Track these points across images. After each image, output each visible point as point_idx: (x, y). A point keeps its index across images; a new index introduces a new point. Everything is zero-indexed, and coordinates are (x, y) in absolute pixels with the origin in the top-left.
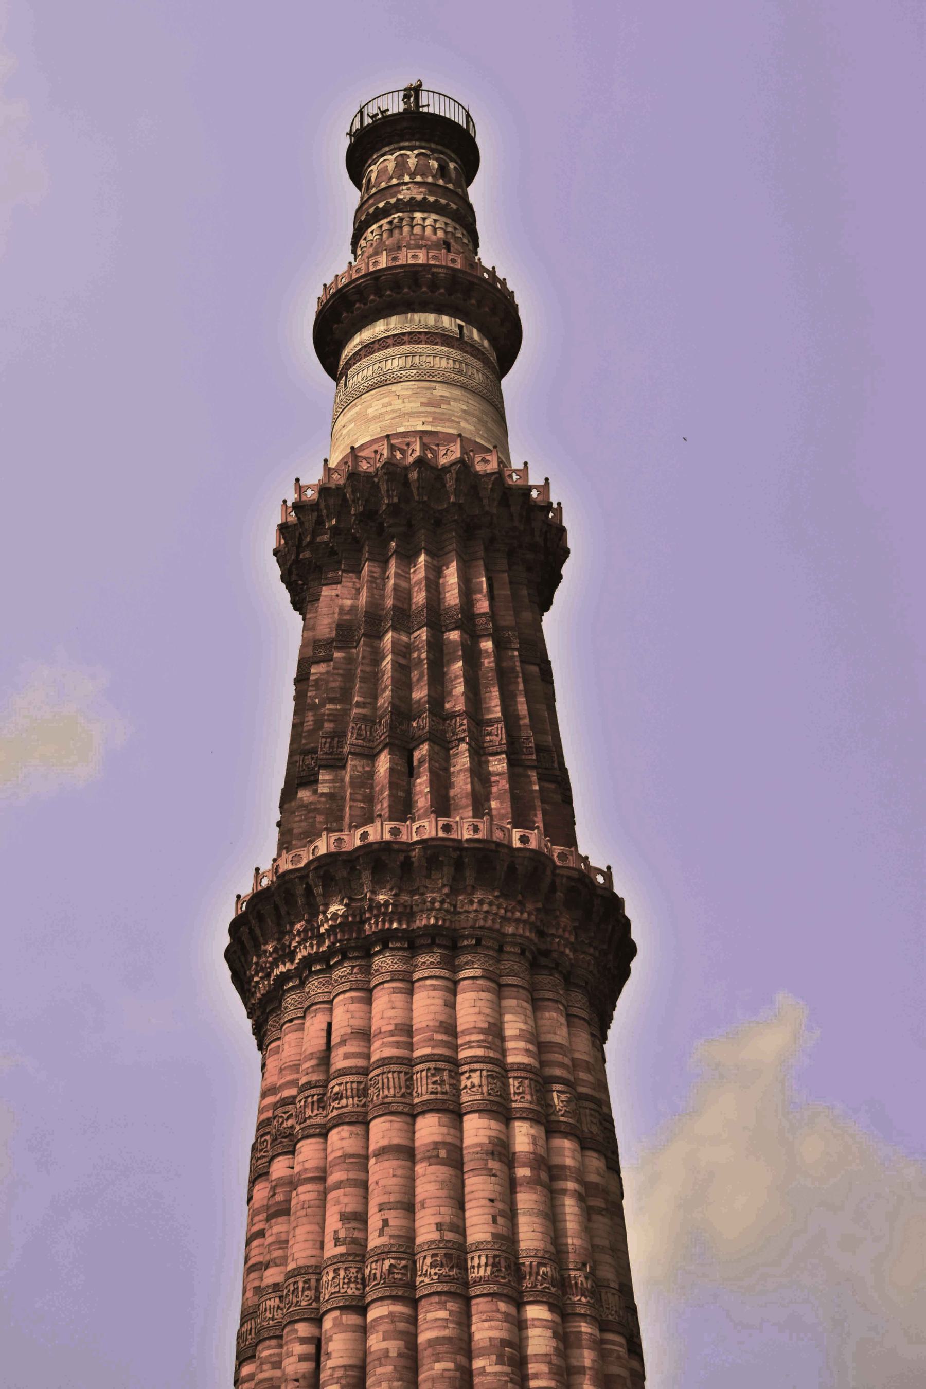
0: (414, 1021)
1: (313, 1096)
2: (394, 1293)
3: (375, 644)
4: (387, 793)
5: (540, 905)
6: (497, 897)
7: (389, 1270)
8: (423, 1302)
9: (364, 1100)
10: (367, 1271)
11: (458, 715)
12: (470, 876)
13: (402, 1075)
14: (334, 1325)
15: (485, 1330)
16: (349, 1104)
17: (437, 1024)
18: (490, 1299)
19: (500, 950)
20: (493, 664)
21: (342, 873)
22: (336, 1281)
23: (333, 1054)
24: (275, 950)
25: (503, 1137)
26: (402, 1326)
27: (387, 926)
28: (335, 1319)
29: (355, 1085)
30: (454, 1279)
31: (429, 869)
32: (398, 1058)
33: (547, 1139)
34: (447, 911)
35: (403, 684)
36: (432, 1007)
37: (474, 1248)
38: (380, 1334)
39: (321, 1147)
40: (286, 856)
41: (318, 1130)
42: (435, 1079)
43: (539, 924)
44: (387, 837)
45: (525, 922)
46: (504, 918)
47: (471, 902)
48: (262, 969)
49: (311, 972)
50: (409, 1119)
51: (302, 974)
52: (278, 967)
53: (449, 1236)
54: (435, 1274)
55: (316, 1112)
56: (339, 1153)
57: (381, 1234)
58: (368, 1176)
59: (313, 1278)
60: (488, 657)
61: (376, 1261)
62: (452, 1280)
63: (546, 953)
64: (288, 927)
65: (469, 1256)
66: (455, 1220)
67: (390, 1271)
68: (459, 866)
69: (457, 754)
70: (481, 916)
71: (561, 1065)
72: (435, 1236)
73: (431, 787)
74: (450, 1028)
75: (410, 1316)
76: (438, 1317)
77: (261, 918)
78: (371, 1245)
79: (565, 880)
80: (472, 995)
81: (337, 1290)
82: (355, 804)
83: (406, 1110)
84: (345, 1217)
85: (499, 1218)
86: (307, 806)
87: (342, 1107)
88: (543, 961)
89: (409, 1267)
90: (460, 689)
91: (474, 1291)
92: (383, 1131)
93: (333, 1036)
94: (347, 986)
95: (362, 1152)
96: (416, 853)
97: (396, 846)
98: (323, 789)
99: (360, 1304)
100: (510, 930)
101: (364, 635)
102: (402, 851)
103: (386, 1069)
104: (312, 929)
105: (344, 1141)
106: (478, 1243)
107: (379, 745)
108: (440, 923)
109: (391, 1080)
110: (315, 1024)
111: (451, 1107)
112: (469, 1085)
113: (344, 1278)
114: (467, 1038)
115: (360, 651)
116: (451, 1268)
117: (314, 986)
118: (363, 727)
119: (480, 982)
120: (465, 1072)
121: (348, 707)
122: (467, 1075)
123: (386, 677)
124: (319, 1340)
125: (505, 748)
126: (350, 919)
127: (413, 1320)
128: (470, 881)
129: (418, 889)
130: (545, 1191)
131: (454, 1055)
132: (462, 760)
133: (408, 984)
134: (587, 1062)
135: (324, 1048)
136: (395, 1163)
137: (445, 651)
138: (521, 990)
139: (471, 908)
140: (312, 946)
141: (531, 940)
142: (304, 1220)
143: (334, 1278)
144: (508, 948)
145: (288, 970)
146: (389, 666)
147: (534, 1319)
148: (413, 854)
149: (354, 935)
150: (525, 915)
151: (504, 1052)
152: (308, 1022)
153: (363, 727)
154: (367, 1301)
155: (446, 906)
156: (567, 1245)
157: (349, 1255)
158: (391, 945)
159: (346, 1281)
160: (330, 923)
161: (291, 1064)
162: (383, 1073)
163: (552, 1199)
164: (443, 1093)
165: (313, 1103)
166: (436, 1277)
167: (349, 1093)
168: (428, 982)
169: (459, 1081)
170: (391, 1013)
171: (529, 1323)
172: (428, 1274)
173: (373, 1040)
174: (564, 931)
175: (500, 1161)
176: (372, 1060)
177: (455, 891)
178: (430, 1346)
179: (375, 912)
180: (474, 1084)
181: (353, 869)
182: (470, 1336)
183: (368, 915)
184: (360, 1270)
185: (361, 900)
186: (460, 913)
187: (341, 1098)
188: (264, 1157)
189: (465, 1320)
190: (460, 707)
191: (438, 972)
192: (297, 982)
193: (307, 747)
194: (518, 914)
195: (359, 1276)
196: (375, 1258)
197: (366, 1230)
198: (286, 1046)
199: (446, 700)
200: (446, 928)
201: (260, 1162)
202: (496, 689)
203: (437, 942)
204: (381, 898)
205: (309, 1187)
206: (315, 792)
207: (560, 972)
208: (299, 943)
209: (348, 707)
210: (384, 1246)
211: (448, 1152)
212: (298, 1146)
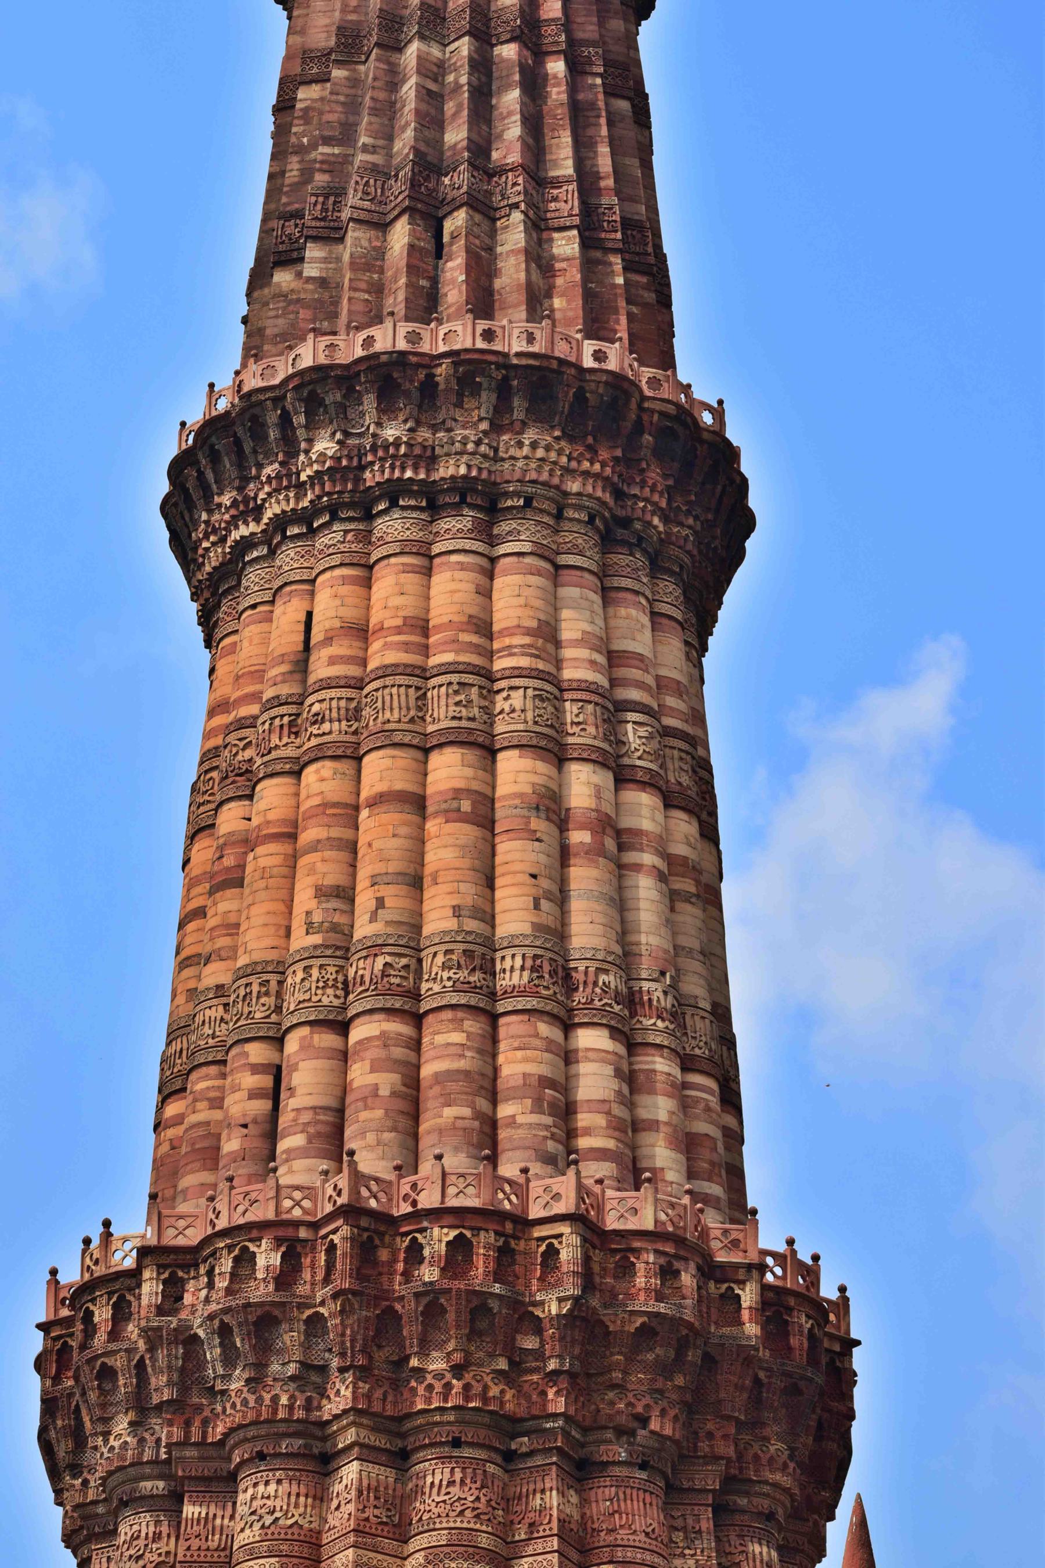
0: (433, 614)
1: (282, 716)
2: (388, 1005)
3: (392, 59)
4: (403, 281)
5: (619, 453)
6: (557, 438)
7: (383, 971)
8: (430, 1019)
9: (356, 725)
11: (511, 170)
12: (519, 406)
13: (412, 691)
14: (302, 1048)
15: (517, 1064)
16: (335, 730)
17: (465, 619)
18: (526, 1017)
19: (559, 516)
20: (564, 97)
21: (334, 396)
22: (307, 984)
23: (312, 659)
24: (235, 503)
25: (555, 788)
26: (399, 1052)
27: (397, 474)
28: (303, 1039)
29: (343, 703)
30: (476, 987)
31: (460, 395)
32: (406, 666)
33: (617, 790)
34: (485, 456)
35: (432, 120)
36: (457, 595)
37: (505, 944)
38: (367, 1063)
39: (292, 790)
40: (254, 367)
41: (288, 766)
42: (458, 698)
43: (616, 479)
44: (402, 345)
45: (597, 476)
46: (567, 470)
47: (520, 444)
48: (215, 531)
49: (284, 537)
50: (419, 755)
51: (271, 539)
52: (237, 527)
53: (471, 925)
54: (449, 979)
55: (285, 740)
56: (316, 801)
57: (373, 918)
58: (357, 834)
59: (274, 979)
60: (558, 85)
61: (366, 957)
62: (474, 989)
63: (625, 523)
64: (254, 471)
65: (499, 955)
66: (480, 902)
67: (384, 974)
68: (504, 392)
69: (507, 227)
70: (533, 466)
71: (640, 685)
72: (452, 924)
73: (468, 275)
74: (483, 627)
75: (411, 1038)
77: (215, 458)
78: (357, 935)
79: (656, 417)
80: (517, 579)
81: (307, 996)
82: (357, 295)
83: (415, 742)
84: (321, 893)
85: (543, 901)
86: (286, 296)
87: (324, 734)
88: (620, 533)
89: (412, 967)
90: (513, 131)
91: (501, 1007)
92: (381, 770)
93: (314, 632)
94: (337, 560)
95: (350, 800)
96: (442, 370)
97: (414, 359)
98: (311, 270)
99: (340, 1018)
100: (574, 486)
101: (377, 44)
102: (424, 366)
103: (389, 681)
104: (289, 476)
105: (324, 783)
106: (512, 936)
107: (394, 209)
108: (474, 473)
109: (395, 697)
110: (288, 614)
111: (480, 740)
112: (507, 709)
113: (318, 981)
114: (507, 641)
115: (370, 68)
116: (474, 970)
117: (289, 557)
118: (372, 181)
119: (528, 560)
120: (503, 689)
121: (351, 151)
122: (505, 694)
123: (407, 109)
124: (279, 1068)
125: (577, 220)
126: (344, 463)
127: (416, 1045)
128: (518, 414)
129: (444, 422)
131: (488, 666)
132: (514, 234)
133: (426, 561)
134: (679, 682)
135: (301, 647)
136: (397, 817)
137: (494, 75)
138: (586, 575)
139: (518, 453)
140: (287, 500)
141: (604, 503)
142: (262, 895)
143: (303, 980)
144: (570, 513)
145: (252, 534)
146: (412, 94)
147: (588, 1050)
148: (439, 371)
149: (350, 486)
150: (597, 467)
151: (558, 663)
152: (278, 609)
153: (372, 181)
154: (349, 1015)
155: (483, 448)
156: (638, 944)
157: (327, 947)
158: (401, 503)
159: (321, 984)
160: (316, 467)
161: (253, 669)
162: (385, 687)
163: (620, 877)
164: (469, 719)
165: (282, 726)
166: (450, 984)
167: (334, 715)
168: (454, 558)
169: (493, 703)
170: (398, 601)
171: (581, 1054)
172: (438, 981)
173: (370, 639)
174: (653, 489)
175: (548, 819)
176: (370, 667)
177: (496, 428)
178: (438, 1082)
179: (380, 453)
180: (515, 708)
181: (351, 390)
182: (496, 1070)
183: (370, 458)
184: (341, 969)
185: (360, 435)
186: (503, 460)
187: (323, 721)
188: (209, 802)
189: (489, 1046)
190: (514, 158)
191: (468, 544)
192: (265, 551)
193: (288, 208)
194: (586, 465)
195: (341, 978)
196: (364, 953)
197: (353, 912)
198: (245, 644)
199: (494, 146)
200: (483, 481)
201: (202, 809)
202: (568, 133)
203: (469, 500)
204: (391, 432)
205: (272, 847)
206: (299, 274)
207: (644, 551)
208: (269, 494)
209: (351, 151)
211: (474, 804)
212: (258, 788)
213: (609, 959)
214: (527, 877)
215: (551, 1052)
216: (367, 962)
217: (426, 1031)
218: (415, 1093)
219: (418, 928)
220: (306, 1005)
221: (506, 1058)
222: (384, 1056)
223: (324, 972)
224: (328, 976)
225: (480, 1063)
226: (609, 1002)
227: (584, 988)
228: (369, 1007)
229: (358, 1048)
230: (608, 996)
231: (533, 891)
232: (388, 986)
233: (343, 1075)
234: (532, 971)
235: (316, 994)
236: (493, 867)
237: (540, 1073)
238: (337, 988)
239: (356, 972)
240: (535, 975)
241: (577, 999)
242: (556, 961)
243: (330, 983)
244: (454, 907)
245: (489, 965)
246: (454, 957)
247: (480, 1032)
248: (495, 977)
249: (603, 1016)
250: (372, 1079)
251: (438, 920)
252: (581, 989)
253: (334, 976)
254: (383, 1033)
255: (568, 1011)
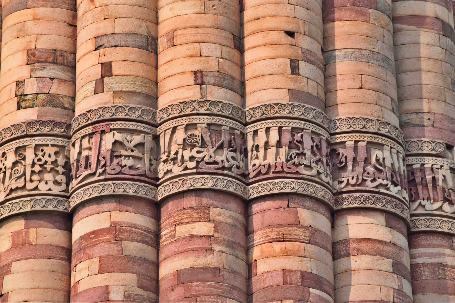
2: (119, 192)
7: (112, 151)
8: (170, 207)
10: (74, 153)
14: (15, 246)
18: (284, 203)
22: (20, 168)
26: (133, 248)
28: (16, 235)
30: (223, 168)
37: (258, 117)
38: (95, 262)
53: (217, 94)
54: (192, 158)
57: (99, 88)
61: (91, 135)
65: (250, 129)
67: (114, 155)
72: (193, 93)
75: (147, 230)
76: (194, 232)
78: (80, 109)
81: (20, 183)
84: (33, 58)
85: (302, 64)
99: (61, 209)
106: (266, 106)
113: (33, 165)
116: (221, 147)
130: (385, 19)
143: (15, 164)
147: (359, 240)
154: (73, 205)
156: (419, 112)
157: (43, 123)
159: (37, 168)
163: (395, 32)
166: (192, 164)
171: (352, 246)
182: (250, 266)
195: (61, 161)
196: (89, 130)
197: (74, 82)
210: (103, 109)
213: (383, 132)
214: (283, 35)
215: (316, 244)
216: (93, 140)
217: (164, 222)
218: (153, 295)
219: (153, 99)
220: (20, 193)
221: (262, 252)
222: (115, 253)
223: (40, 154)
224: (46, 158)
225: (231, 258)
226: (385, 182)
227: (354, 166)
228: (96, 195)
229: (84, 243)
230: (382, 175)
231: (290, 51)
232: (118, 169)
233: (66, 277)
234: (290, 148)
235: (31, 181)
236: (242, 24)
237: (303, 269)
238: (57, 172)
239: (80, 153)
240: (295, 151)
241: (345, 180)
242: (319, 135)
243: (49, 167)
244: (195, 73)
245: (239, 141)
246: (197, 133)
247: (230, 221)
248: (246, 156)
249: (377, 200)
250: (101, 280)
251: (176, 90)
252: (350, 168)
253: (53, 158)
254: (114, 226)
255: (334, 194)
